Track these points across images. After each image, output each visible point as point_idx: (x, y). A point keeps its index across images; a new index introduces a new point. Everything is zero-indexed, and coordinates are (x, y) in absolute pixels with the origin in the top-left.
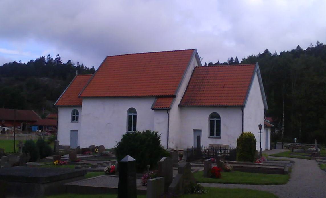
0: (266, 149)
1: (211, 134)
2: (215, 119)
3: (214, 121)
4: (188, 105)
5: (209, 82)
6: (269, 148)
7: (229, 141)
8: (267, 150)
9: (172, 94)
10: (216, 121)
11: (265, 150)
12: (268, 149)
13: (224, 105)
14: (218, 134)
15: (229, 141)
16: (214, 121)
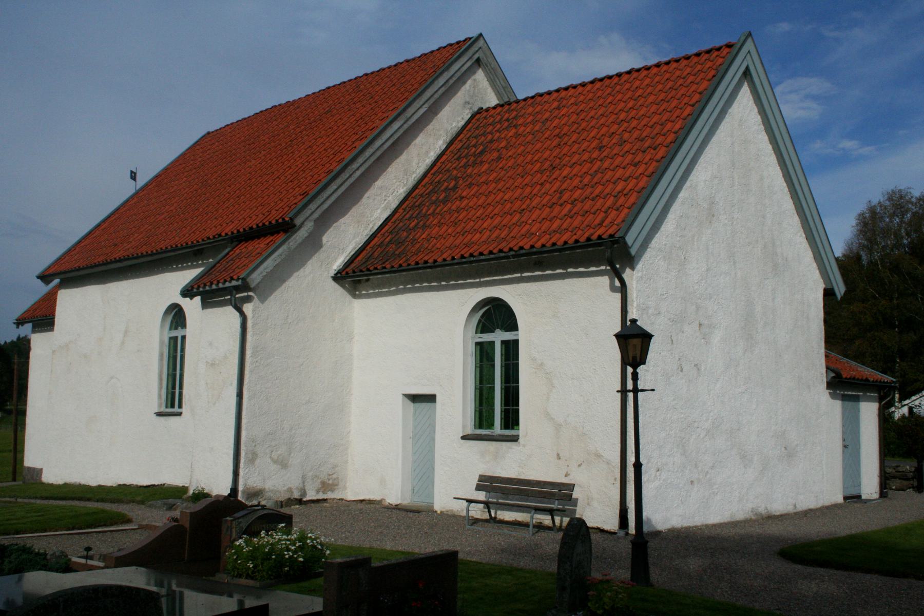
0: (845, 498)
1: (483, 418)
2: (498, 337)
3: (492, 343)
4: (368, 270)
5: (499, 158)
6: (870, 486)
7: (559, 457)
8: (853, 498)
9: (274, 217)
10: (503, 342)
11: (840, 499)
12: (863, 497)
13: (521, 248)
14: (511, 419)
15: (559, 457)
16: (492, 343)
